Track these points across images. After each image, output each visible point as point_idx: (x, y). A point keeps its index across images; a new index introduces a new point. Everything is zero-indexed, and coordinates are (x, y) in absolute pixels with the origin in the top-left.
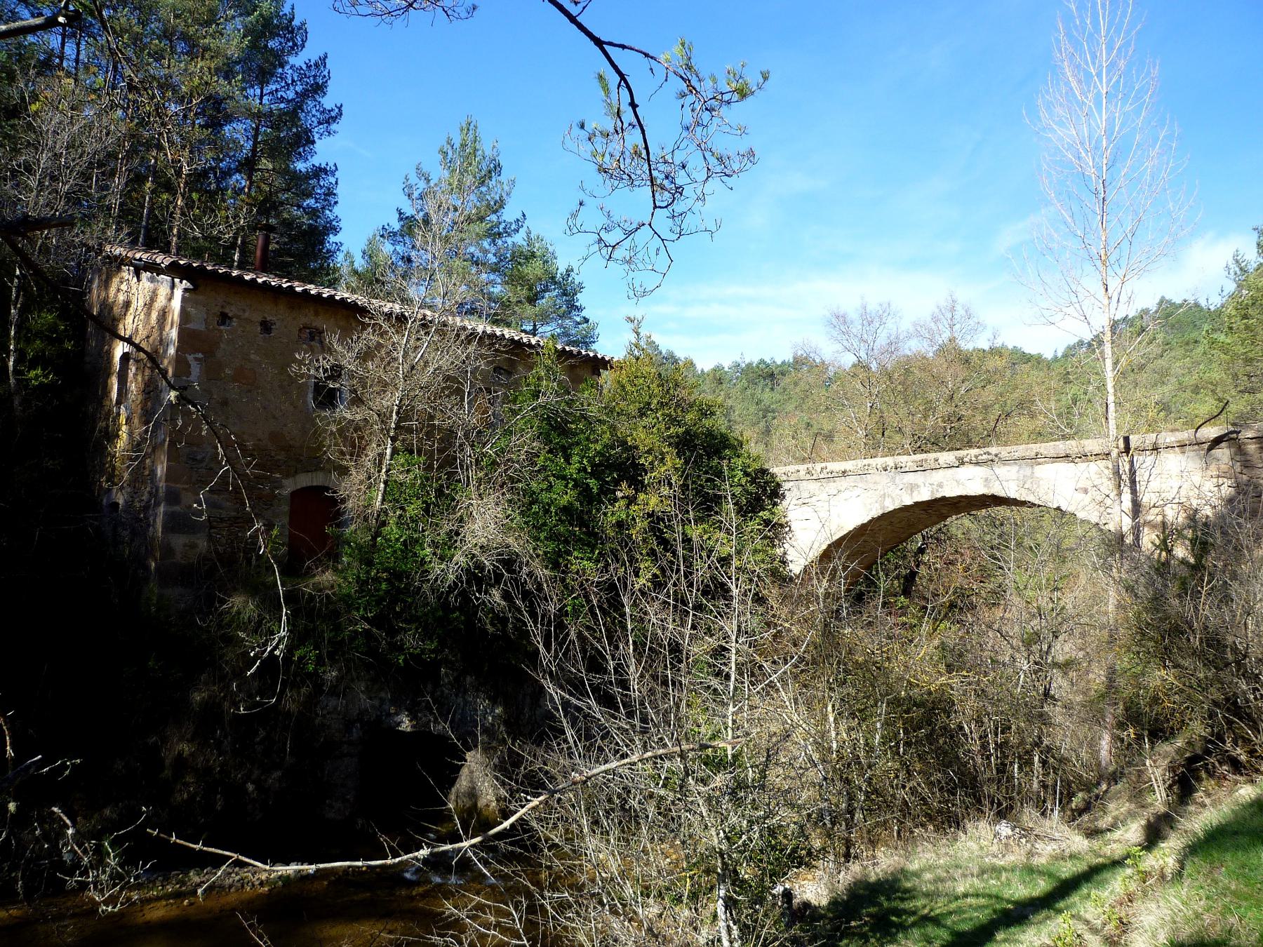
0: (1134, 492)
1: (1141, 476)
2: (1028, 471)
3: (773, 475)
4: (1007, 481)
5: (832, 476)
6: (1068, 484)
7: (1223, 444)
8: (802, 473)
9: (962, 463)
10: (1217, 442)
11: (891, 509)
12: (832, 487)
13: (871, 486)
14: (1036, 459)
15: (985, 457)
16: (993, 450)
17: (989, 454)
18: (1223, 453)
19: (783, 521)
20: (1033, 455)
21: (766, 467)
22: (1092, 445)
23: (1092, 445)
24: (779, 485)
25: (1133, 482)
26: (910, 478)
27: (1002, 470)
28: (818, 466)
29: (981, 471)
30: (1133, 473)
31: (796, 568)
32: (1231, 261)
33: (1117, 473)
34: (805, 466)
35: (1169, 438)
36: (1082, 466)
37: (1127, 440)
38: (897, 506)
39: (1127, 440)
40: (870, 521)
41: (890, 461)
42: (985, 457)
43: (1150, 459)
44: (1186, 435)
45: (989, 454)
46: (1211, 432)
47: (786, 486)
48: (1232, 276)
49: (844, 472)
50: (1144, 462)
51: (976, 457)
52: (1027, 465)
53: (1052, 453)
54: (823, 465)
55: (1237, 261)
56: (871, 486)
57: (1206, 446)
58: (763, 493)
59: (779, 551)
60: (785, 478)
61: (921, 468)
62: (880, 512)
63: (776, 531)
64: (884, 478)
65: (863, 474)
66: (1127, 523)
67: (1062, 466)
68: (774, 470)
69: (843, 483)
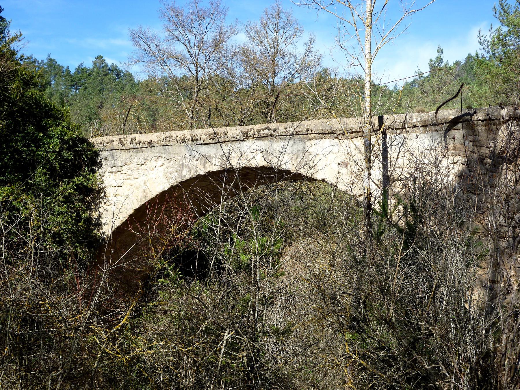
0: (385, 168)
1: (393, 152)
2: (300, 146)
3: (89, 144)
4: (285, 156)
5: (140, 147)
6: (332, 161)
7: (460, 126)
8: (116, 143)
9: (246, 137)
10: (454, 123)
11: (188, 177)
12: (139, 158)
13: (172, 156)
14: (307, 134)
15: (266, 131)
16: (273, 126)
17: (269, 129)
18: (458, 133)
19: (101, 186)
20: (304, 131)
21: (84, 134)
22: (352, 123)
23: (352, 123)
24: (96, 154)
25: (385, 158)
26: (204, 150)
27: (277, 145)
28: (129, 137)
29: (262, 144)
30: (385, 151)
31: (107, 230)
32: (498, 4)
33: (369, 147)
34: (118, 137)
35: (416, 118)
36: (345, 142)
37: (381, 119)
38: (192, 175)
39: (381, 119)
40: (170, 189)
41: (187, 133)
42: (266, 131)
43: (399, 138)
44: (428, 116)
45: (269, 129)
46: (449, 113)
47: (103, 155)
48: (498, 15)
49: (150, 143)
50: (394, 140)
51: (258, 131)
52: (300, 140)
53: (320, 130)
54: (133, 136)
55: (502, 5)
56: (172, 156)
57: (445, 126)
58: (83, 159)
59: (95, 215)
60: (101, 147)
61: (216, 141)
62: (179, 181)
63: (91, 195)
64: (182, 150)
65: (165, 144)
66: (377, 192)
67: (327, 142)
68: (93, 140)
69: (150, 153)
